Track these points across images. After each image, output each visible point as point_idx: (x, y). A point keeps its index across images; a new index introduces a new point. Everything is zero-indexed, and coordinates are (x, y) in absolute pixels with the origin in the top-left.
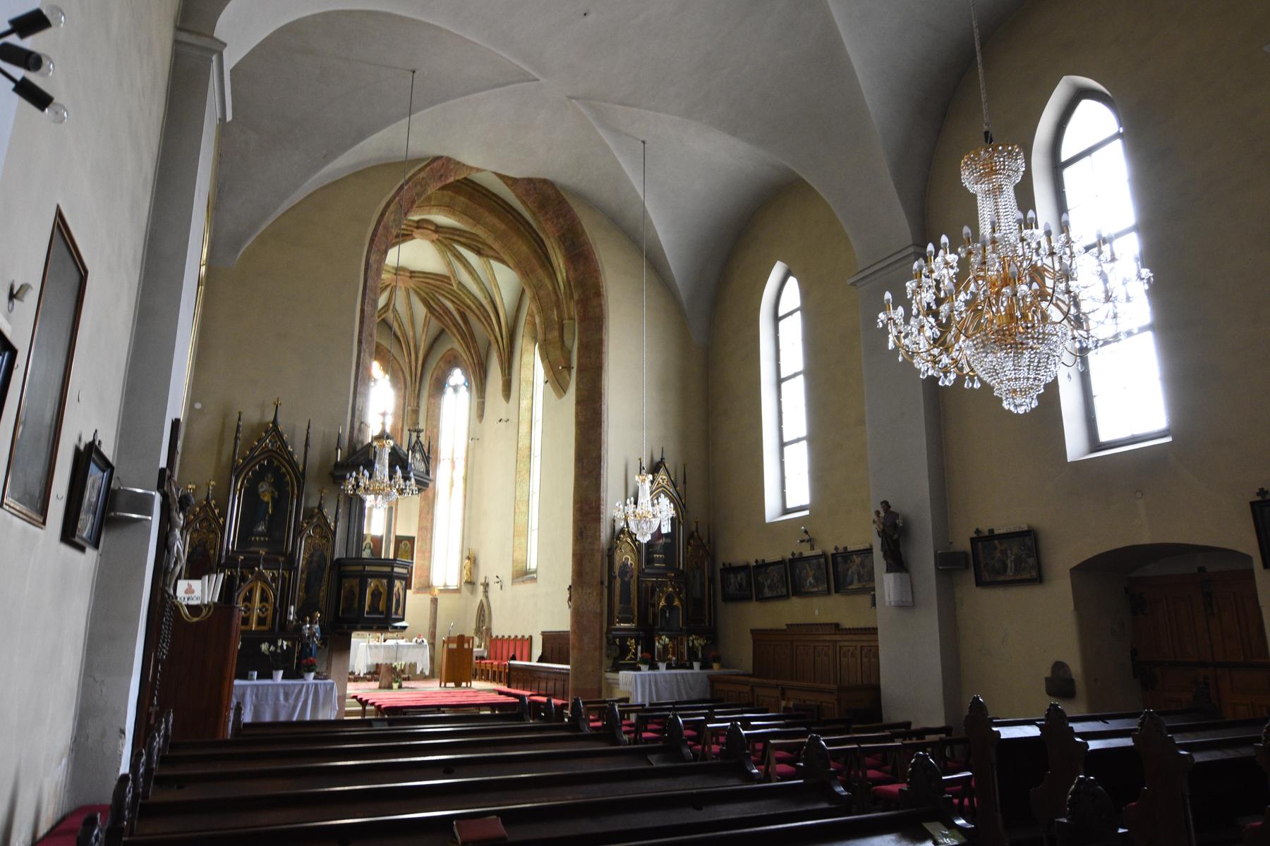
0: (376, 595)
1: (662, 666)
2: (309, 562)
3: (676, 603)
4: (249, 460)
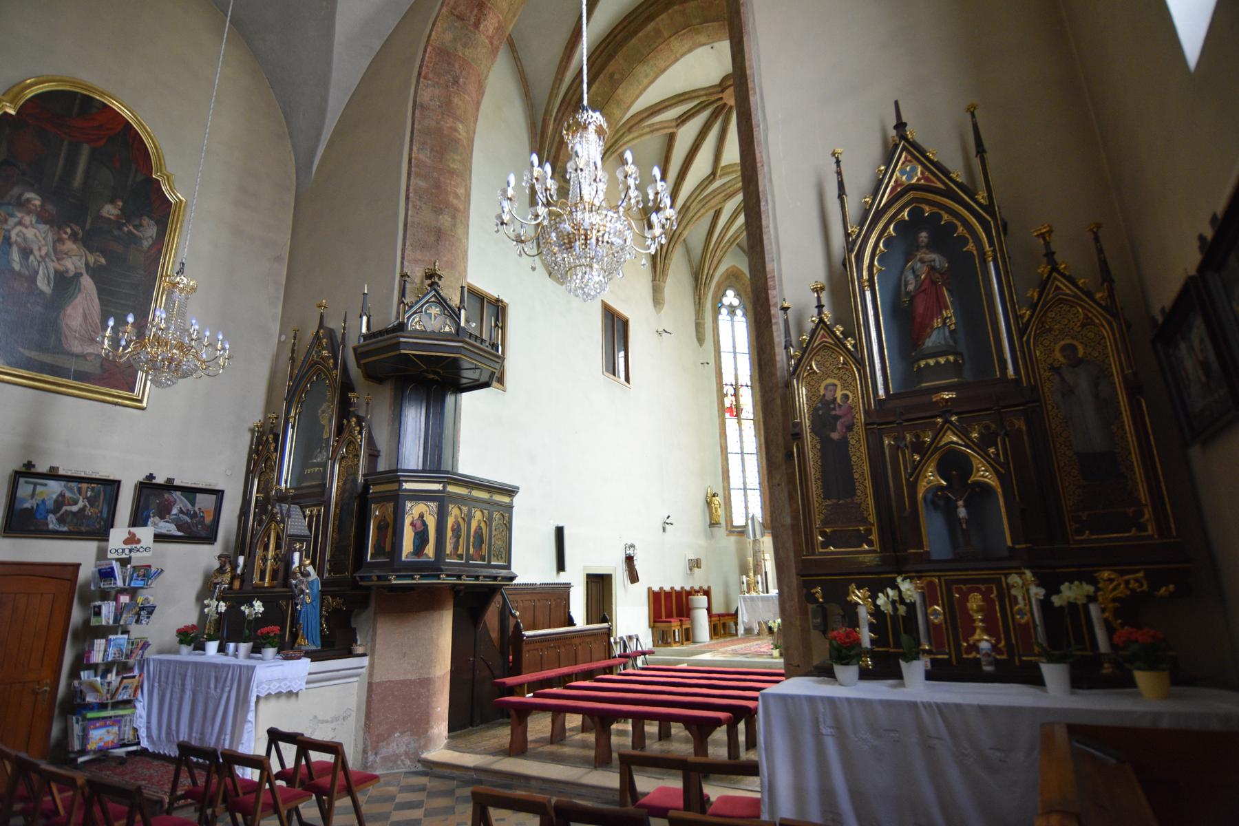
0: (381, 528)
3: (984, 474)
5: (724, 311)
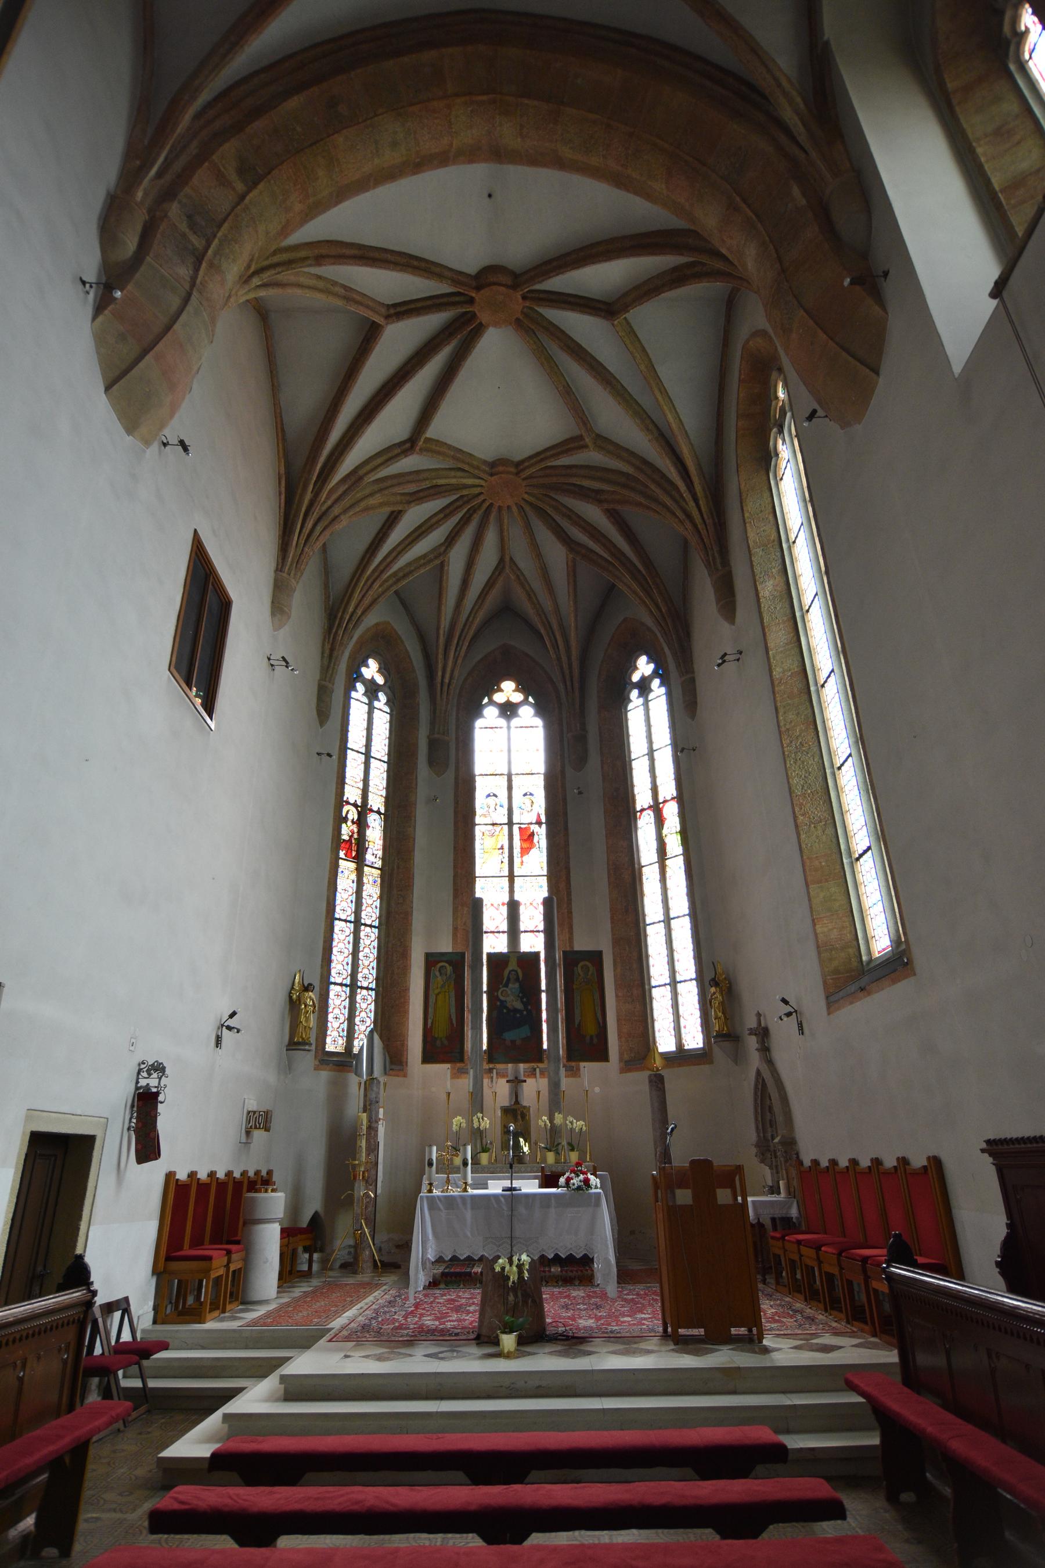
5: (360, 687)
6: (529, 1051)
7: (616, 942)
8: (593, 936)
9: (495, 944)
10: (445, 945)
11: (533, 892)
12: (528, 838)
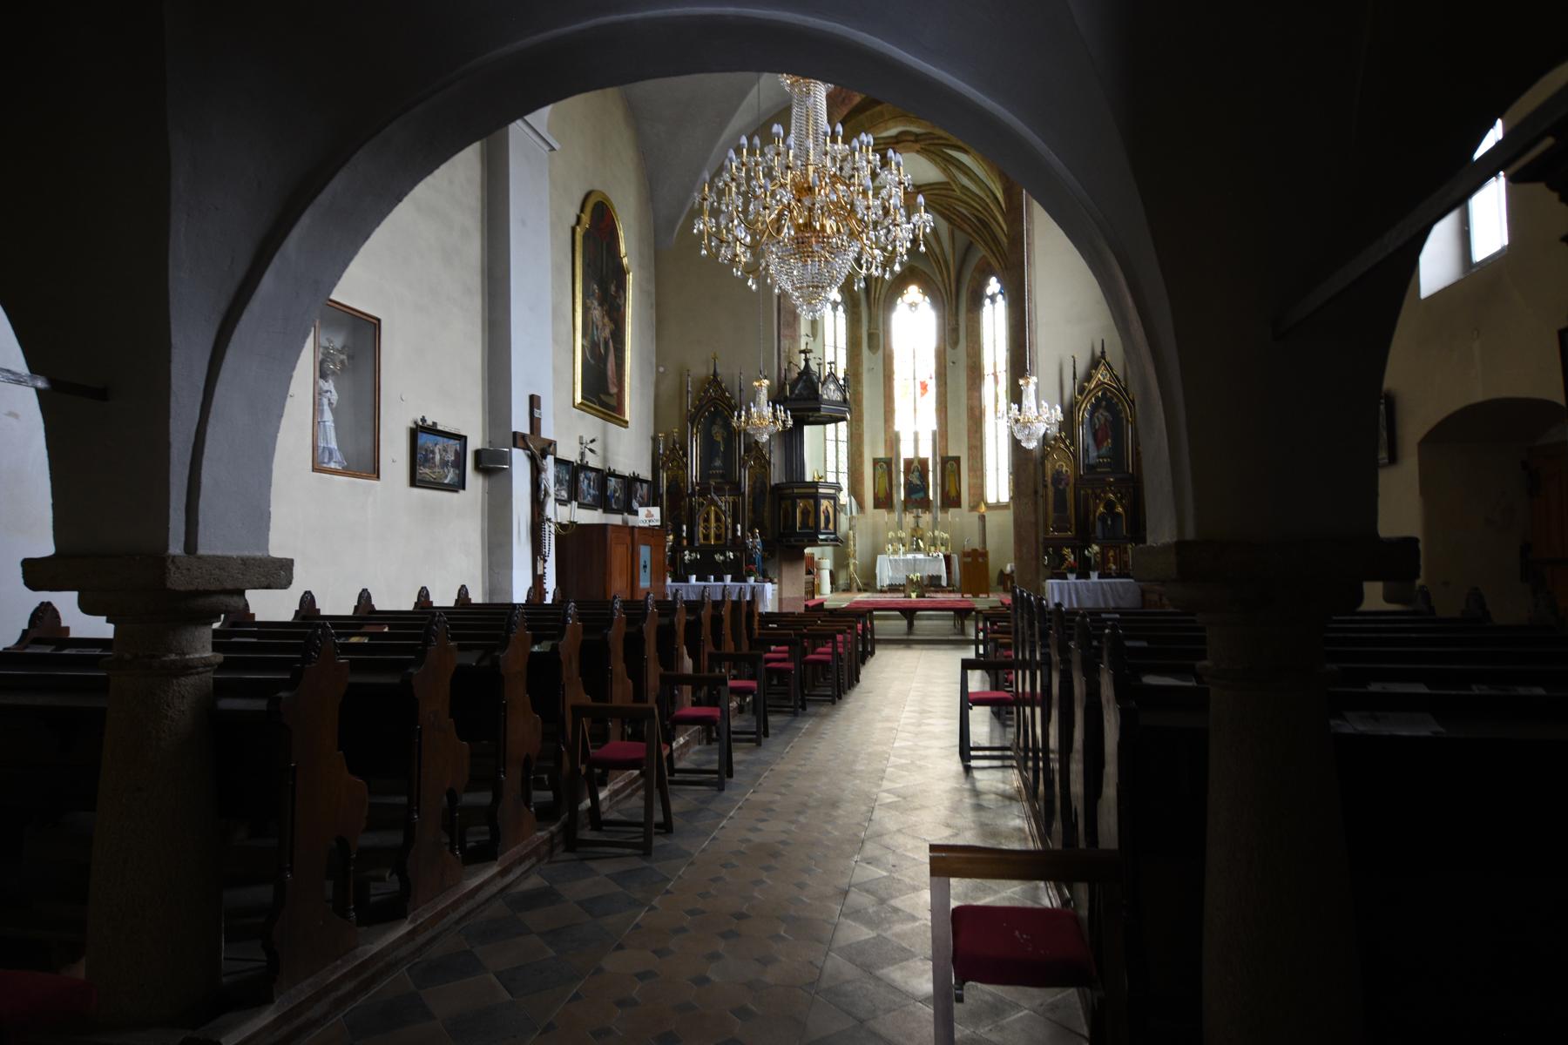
0: (805, 513)
1: (1094, 576)
2: (753, 488)
3: (1120, 509)
4: (699, 409)
6: (925, 504)
7: (970, 448)
8: (958, 449)
9: (906, 452)
10: (881, 454)
11: (927, 421)
12: (924, 387)
